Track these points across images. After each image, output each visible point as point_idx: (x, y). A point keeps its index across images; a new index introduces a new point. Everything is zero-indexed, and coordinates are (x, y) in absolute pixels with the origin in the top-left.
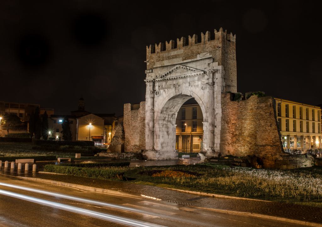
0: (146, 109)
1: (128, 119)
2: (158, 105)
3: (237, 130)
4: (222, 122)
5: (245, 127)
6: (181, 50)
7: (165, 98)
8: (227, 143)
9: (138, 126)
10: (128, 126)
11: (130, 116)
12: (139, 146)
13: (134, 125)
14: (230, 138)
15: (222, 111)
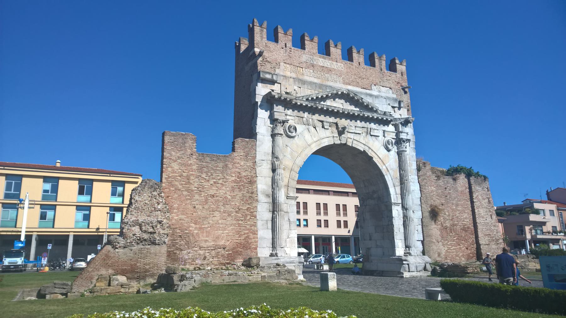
0: (259, 157)
1: (185, 174)
2: (291, 154)
5: (457, 217)
6: (339, 64)
8: (434, 241)
9: (229, 197)
10: (185, 193)
11: (194, 167)
12: (234, 248)
13: (212, 192)
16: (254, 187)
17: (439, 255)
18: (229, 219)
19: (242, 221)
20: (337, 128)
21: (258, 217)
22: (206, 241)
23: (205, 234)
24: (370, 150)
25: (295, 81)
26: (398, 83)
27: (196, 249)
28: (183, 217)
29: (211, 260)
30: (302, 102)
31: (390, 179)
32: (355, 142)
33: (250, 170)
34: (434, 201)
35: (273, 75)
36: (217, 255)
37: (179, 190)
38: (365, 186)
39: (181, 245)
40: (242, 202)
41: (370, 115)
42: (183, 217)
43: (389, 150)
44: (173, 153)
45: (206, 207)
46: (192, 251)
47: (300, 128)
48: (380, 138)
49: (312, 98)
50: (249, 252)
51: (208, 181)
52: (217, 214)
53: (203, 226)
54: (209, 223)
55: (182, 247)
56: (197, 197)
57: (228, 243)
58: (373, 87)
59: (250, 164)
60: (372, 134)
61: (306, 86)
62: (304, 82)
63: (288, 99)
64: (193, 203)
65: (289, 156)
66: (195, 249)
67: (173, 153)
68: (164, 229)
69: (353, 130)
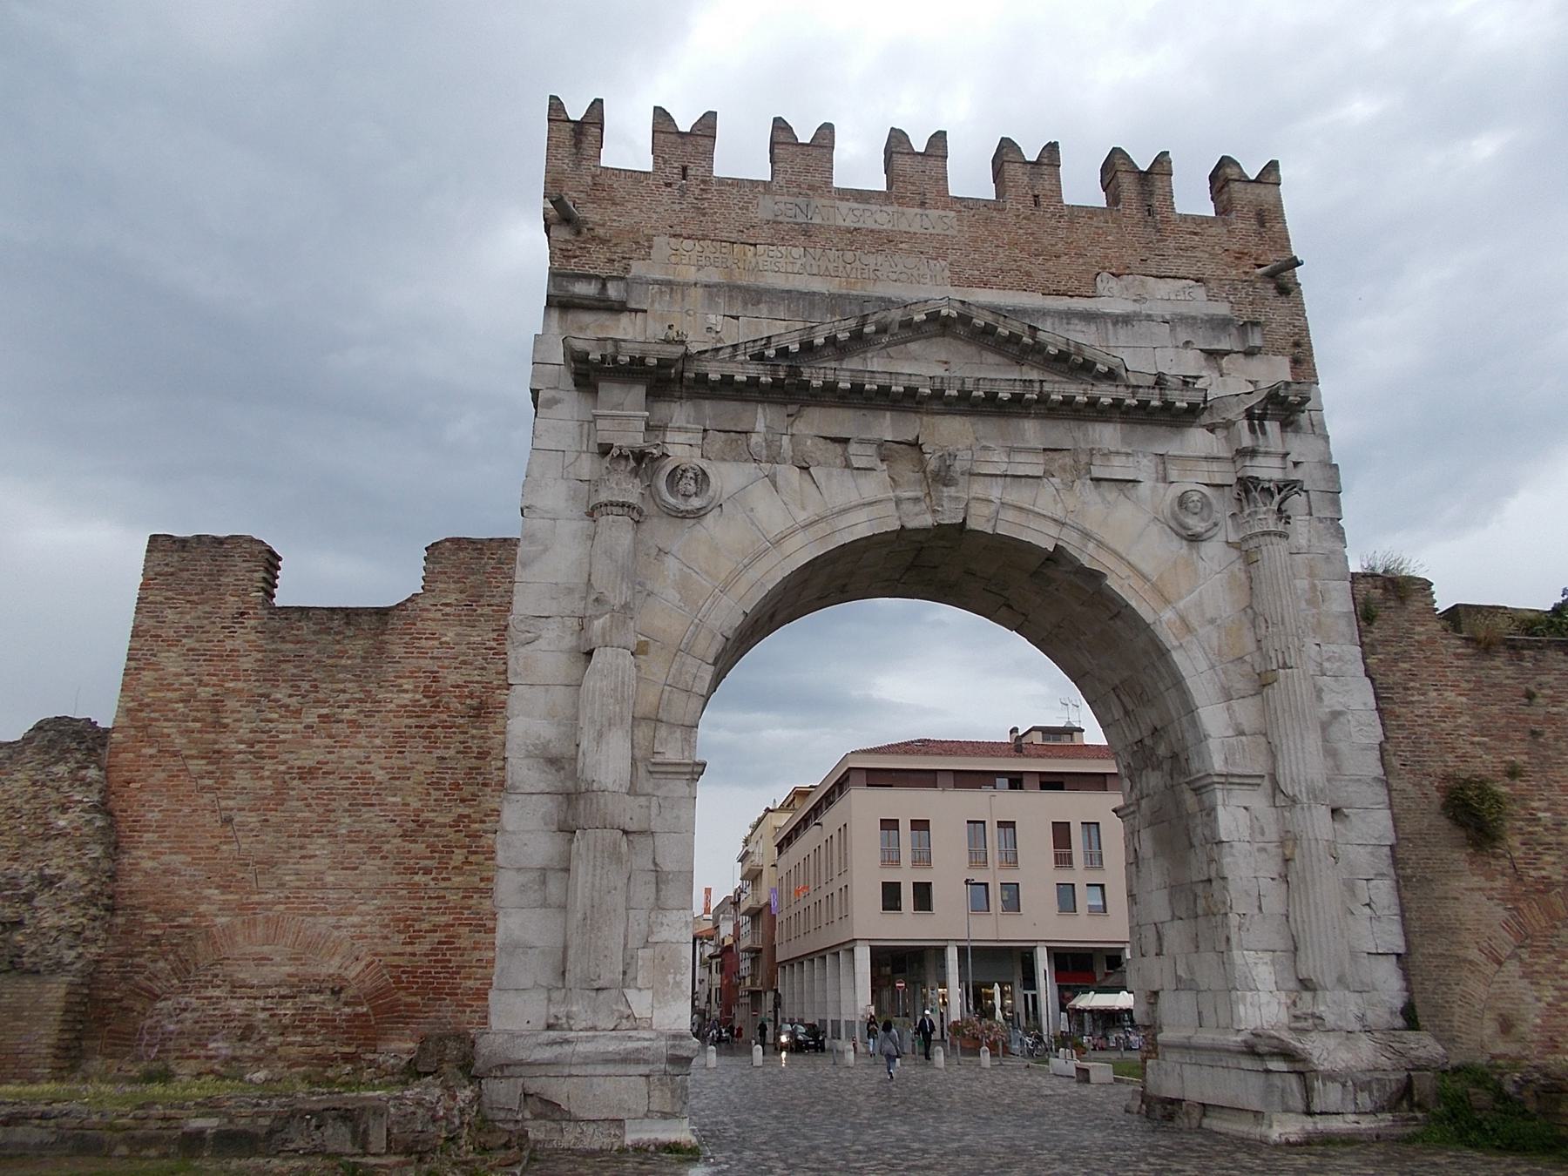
0: (524, 603)
1: (204, 693)
3: (1548, 847)
4: (1395, 783)
7: (777, 542)
8: (1473, 954)
10: (197, 766)
11: (246, 663)
13: (307, 757)
14: (1501, 913)
15: (1377, 698)
16: (492, 728)
17: (1506, 1026)
18: (372, 865)
19: (427, 871)
20: (922, 465)
21: (501, 857)
22: (262, 960)
23: (260, 930)
24: (1091, 545)
25: (711, 297)
26: (1240, 256)
27: (217, 993)
28: (177, 860)
29: (273, 1040)
30: (729, 369)
31: (1203, 665)
32: (1009, 515)
33: (480, 661)
34: (1463, 758)
35: (604, 282)
36: (300, 1023)
37: (175, 754)
38: (1127, 713)
39: (154, 977)
40: (435, 794)
41: (1079, 392)
42: (177, 860)
43: (1194, 539)
44: (170, 615)
45: (274, 817)
46: (196, 1003)
47: (727, 476)
48: (1144, 489)
49: (783, 352)
50: (447, 1009)
51: (299, 712)
52: (319, 846)
53: (256, 898)
54: (282, 885)
55: (157, 987)
56: (243, 778)
57: (354, 971)
58: (1105, 283)
59: (483, 634)
60: (1096, 472)
61: (764, 308)
62: (755, 296)
63: (652, 361)
64: (223, 803)
65: (673, 595)
66: (210, 992)
67: (170, 615)
68: (60, 910)
69: (998, 462)
